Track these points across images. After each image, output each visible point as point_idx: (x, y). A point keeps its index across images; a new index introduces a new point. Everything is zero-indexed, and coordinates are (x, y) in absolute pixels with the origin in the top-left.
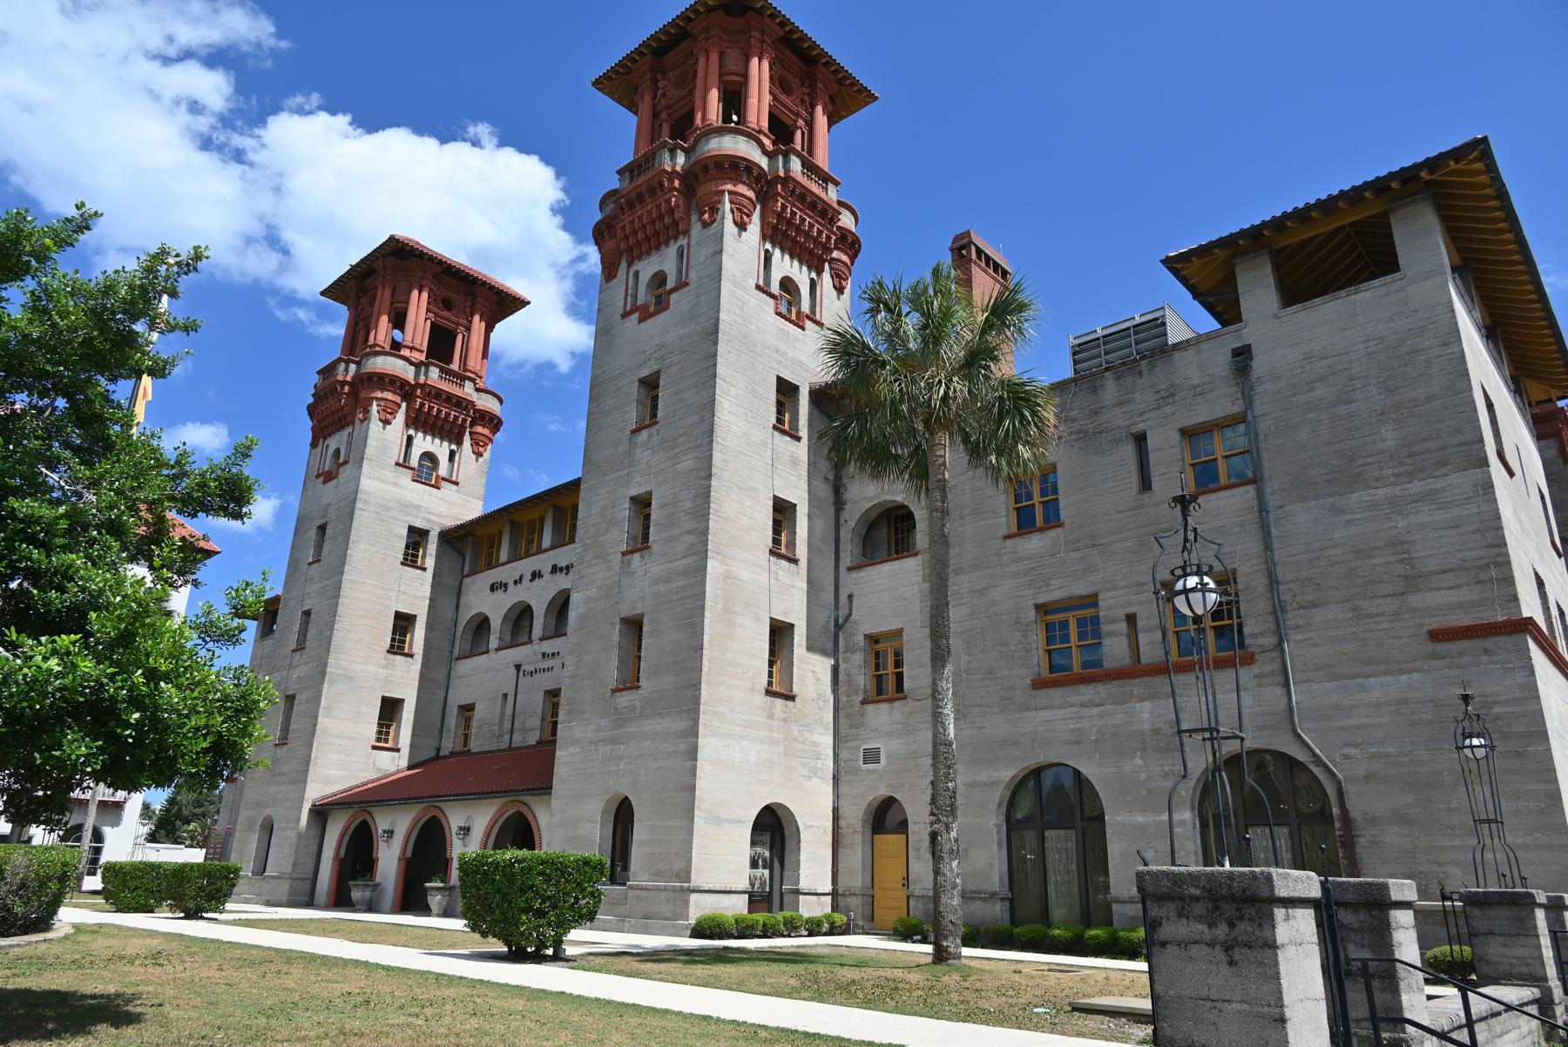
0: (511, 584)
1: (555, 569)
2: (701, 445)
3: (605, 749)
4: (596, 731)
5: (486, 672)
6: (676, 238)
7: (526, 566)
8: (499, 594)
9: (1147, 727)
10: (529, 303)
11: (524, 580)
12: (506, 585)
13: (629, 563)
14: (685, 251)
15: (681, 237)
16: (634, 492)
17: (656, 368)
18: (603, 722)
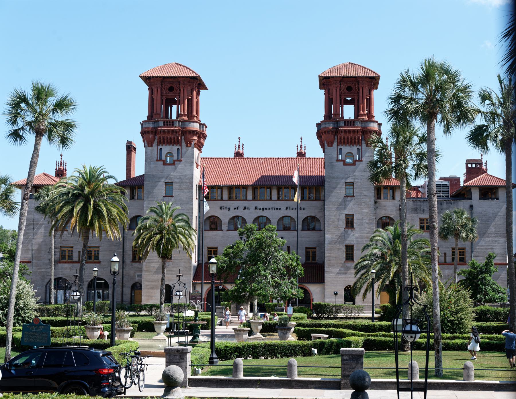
0: (232, 208)
1: (256, 208)
2: (370, 207)
3: (342, 276)
4: (339, 271)
5: (222, 237)
6: (356, 146)
7: (241, 204)
8: (226, 211)
9: (447, 274)
10: (207, 89)
11: (239, 208)
12: (229, 209)
13: (347, 232)
14: (360, 151)
15: (358, 145)
16: (347, 213)
17: (352, 181)
18: (342, 269)
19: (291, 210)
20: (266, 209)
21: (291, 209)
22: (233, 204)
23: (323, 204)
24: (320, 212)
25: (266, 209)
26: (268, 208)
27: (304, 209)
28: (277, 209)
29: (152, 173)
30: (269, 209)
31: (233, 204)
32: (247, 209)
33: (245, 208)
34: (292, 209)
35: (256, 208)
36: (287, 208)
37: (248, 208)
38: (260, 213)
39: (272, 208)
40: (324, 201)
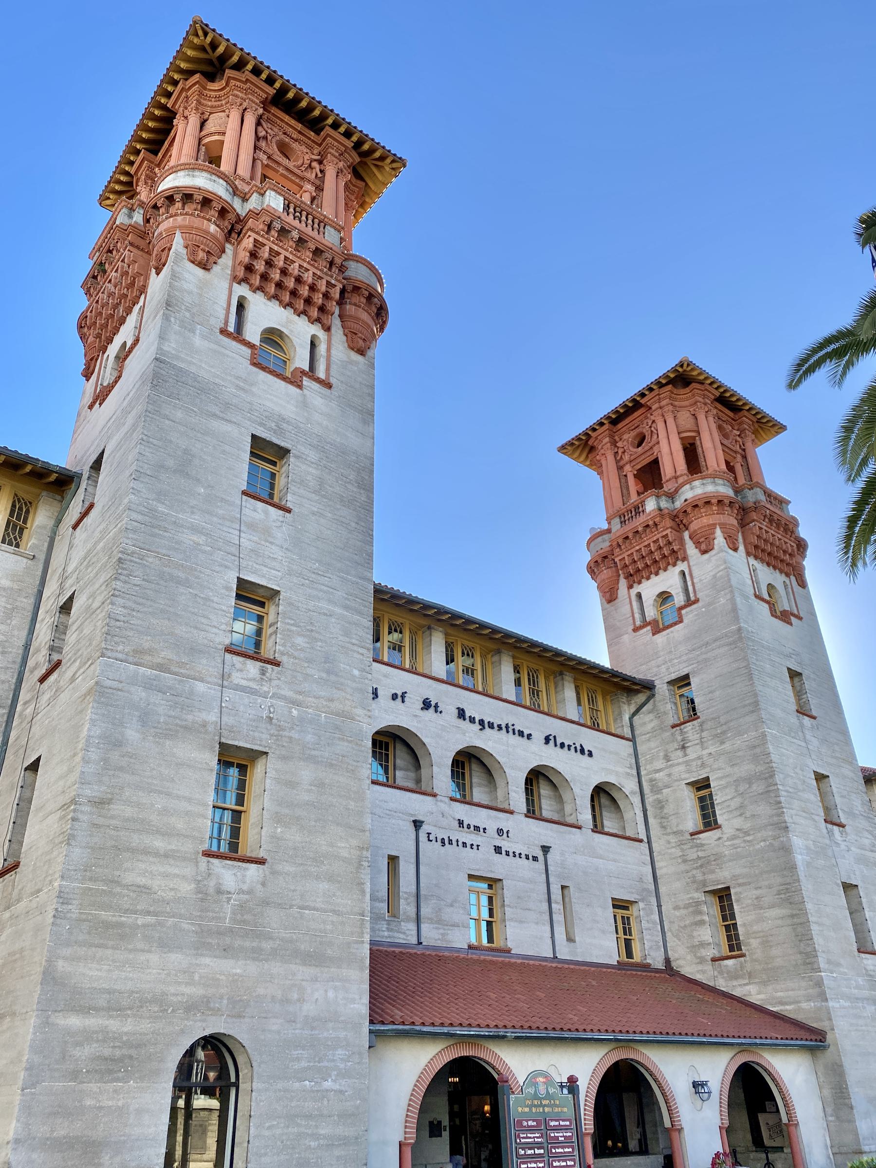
19: (558, 749)
20: (491, 726)
21: (558, 744)
22: (386, 676)
23: (631, 751)
24: (628, 774)
25: (491, 726)
26: (495, 725)
27: (590, 754)
28: (521, 734)
29: (193, 369)
30: (500, 727)
31: (385, 676)
32: (432, 709)
33: (426, 705)
34: (562, 745)
35: (461, 714)
36: (547, 740)
37: (436, 706)
38: (472, 737)
39: (507, 726)
40: (633, 740)
